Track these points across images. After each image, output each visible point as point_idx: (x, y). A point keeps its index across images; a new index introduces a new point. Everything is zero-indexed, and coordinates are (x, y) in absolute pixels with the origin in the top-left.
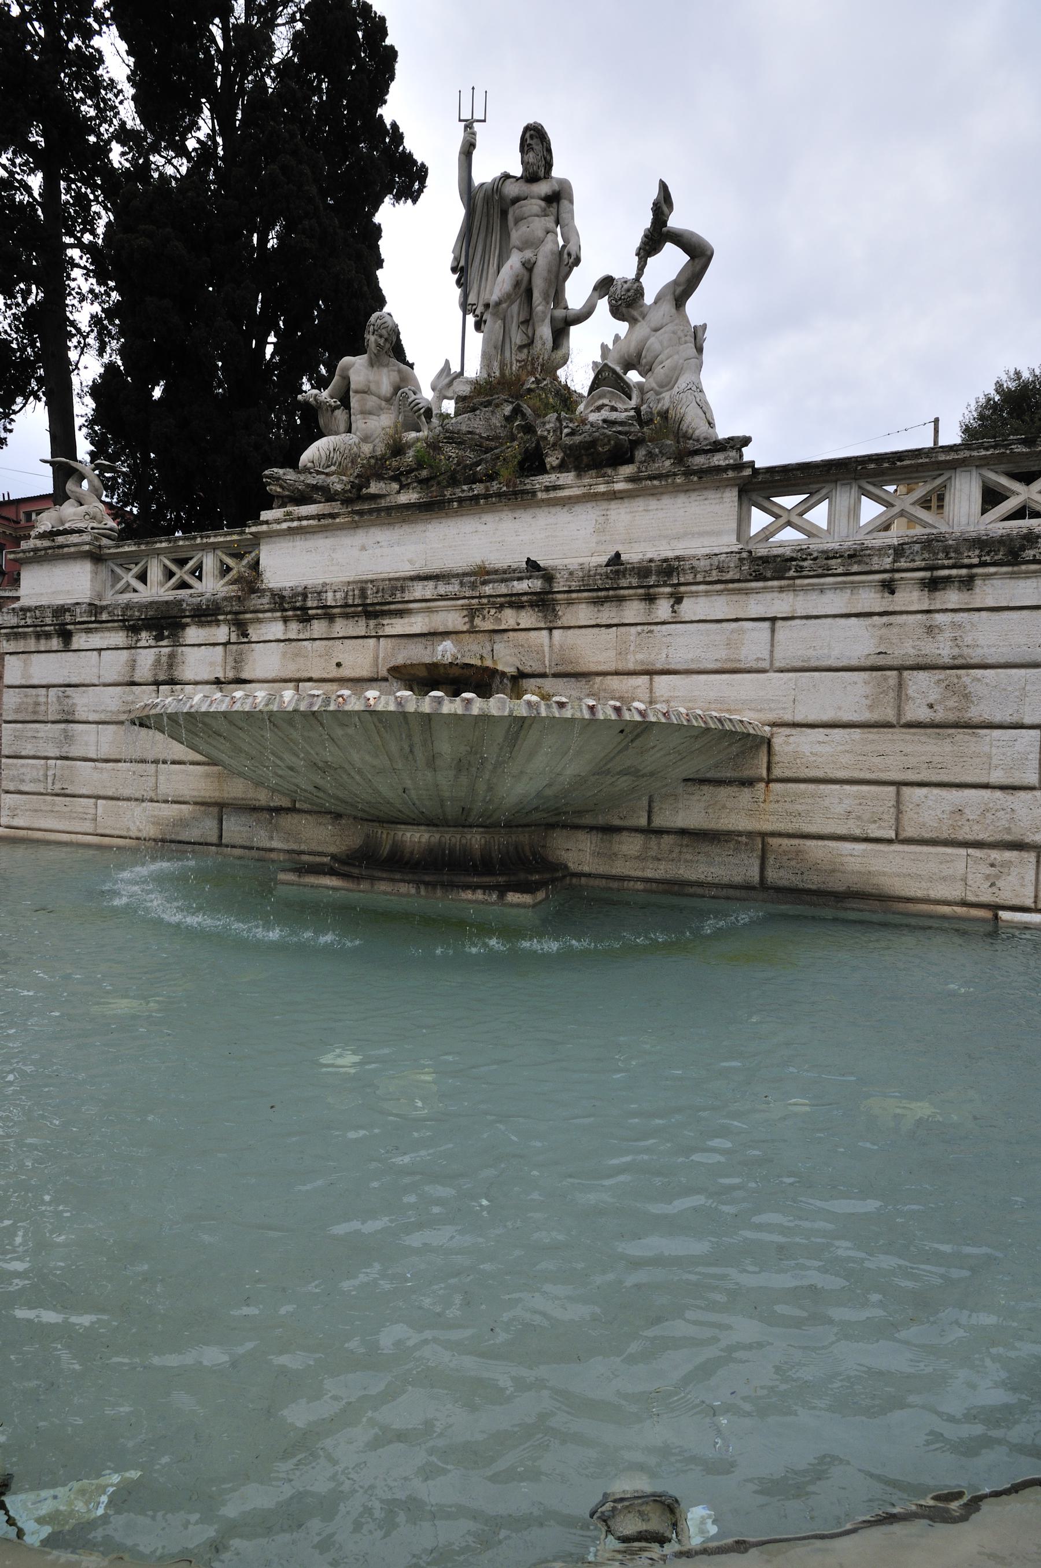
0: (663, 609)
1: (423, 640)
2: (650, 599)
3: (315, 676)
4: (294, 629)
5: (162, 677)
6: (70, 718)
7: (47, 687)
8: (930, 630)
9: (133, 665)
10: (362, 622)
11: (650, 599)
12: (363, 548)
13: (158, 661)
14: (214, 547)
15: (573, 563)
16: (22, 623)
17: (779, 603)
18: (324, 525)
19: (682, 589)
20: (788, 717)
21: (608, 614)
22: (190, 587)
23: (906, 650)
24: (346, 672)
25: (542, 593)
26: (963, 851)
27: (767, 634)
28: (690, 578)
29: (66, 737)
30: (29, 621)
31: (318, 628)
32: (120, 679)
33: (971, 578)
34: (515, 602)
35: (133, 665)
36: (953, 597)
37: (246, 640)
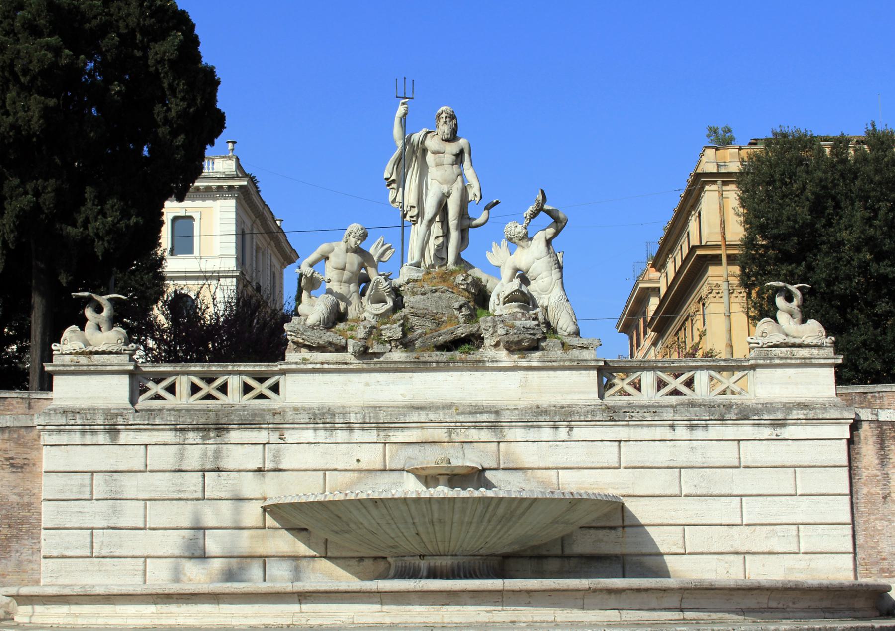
0: (563, 433)
1: (417, 446)
2: (556, 427)
3: (339, 467)
4: (322, 435)
5: (208, 466)
6: (119, 497)
7: (93, 472)
8: (692, 449)
9: (181, 456)
10: (375, 432)
11: (556, 427)
12: (367, 384)
13: (205, 455)
14: (240, 373)
16: (72, 422)
17: (621, 432)
18: (343, 369)
19: (573, 423)
20: (631, 492)
21: (533, 434)
22: (214, 398)
24: (363, 465)
25: (494, 420)
26: (714, 557)
27: (616, 449)
28: (577, 418)
29: (114, 512)
30: (79, 422)
31: (341, 435)
32: (169, 467)
33: (707, 425)
34: (478, 426)
35: (181, 456)
36: (699, 434)
37: (282, 441)
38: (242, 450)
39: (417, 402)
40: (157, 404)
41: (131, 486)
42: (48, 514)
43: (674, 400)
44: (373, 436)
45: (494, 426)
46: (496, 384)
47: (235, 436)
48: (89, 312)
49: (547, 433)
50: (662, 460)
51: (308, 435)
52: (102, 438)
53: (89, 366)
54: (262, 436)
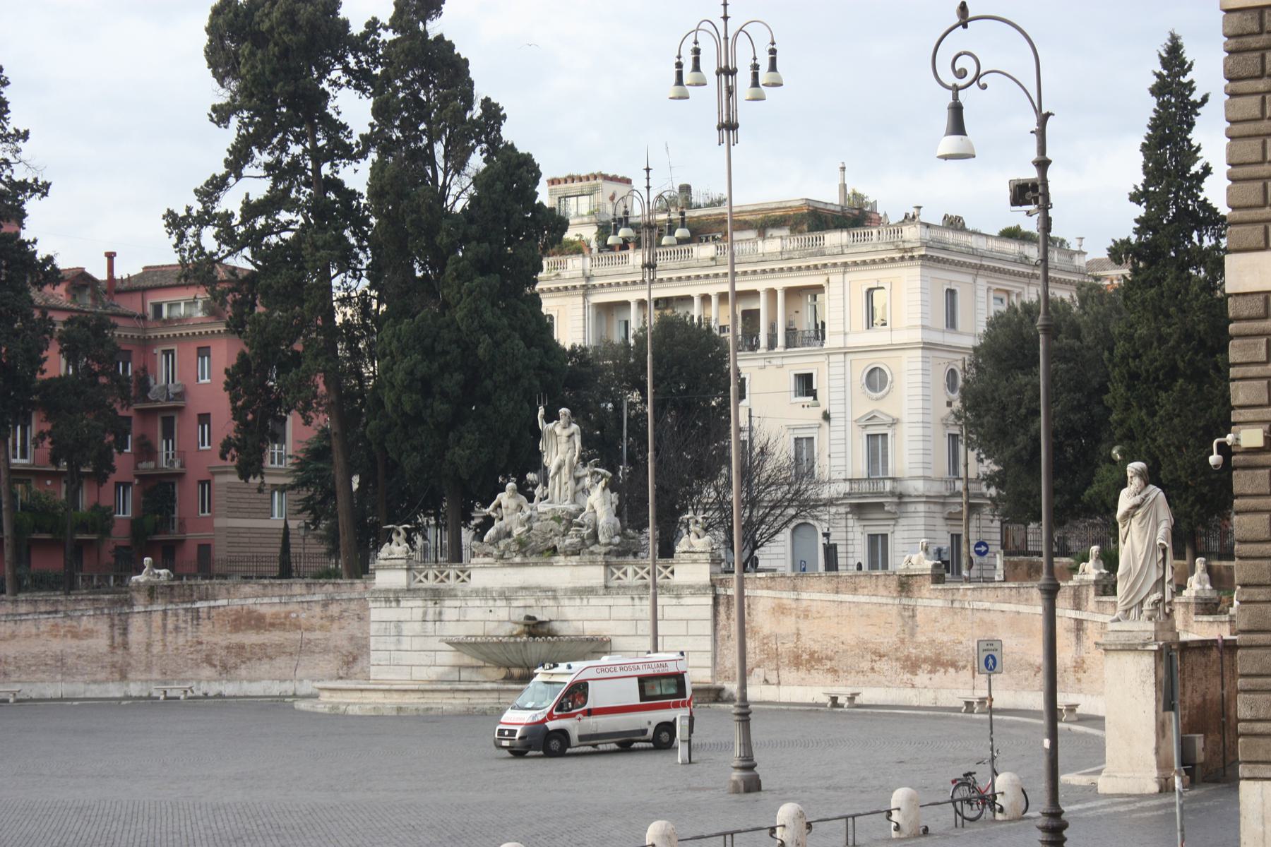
0: (585, 601)
9: (425, 613)
15: (563, 586)
21: (572, 603)
23: (637, 616)
35: (425, 613)
38: (450, 608)
39: (525, 585)
40: (420, 585)
42: (373, 643)
43: (640, 582)
44: (504, 603)
45: (555, 598)
46: (562, 574)
47: (448, 603)
49: (578, 602)
50: (628, 616)
51: (478, 603)
54: (458, 603)
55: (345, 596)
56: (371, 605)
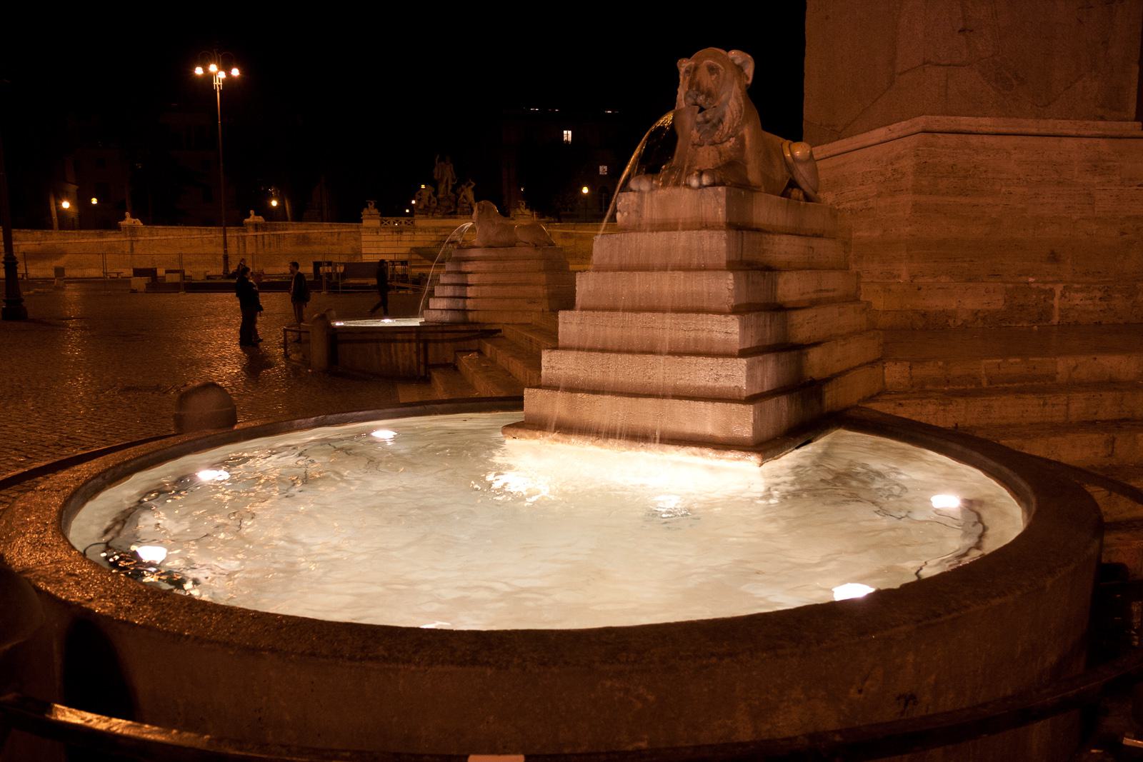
38: (406, 236)
41: (381, 244)
44: (434, 234)
48: (369, 205)
51: (420, 233)
52: (375, 234)
53: (371, 216)
55: (348, 230)
56: (362, 234)
